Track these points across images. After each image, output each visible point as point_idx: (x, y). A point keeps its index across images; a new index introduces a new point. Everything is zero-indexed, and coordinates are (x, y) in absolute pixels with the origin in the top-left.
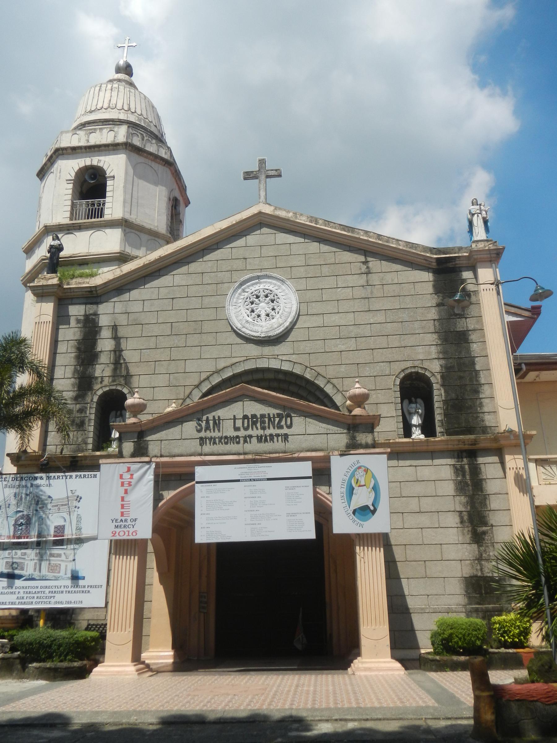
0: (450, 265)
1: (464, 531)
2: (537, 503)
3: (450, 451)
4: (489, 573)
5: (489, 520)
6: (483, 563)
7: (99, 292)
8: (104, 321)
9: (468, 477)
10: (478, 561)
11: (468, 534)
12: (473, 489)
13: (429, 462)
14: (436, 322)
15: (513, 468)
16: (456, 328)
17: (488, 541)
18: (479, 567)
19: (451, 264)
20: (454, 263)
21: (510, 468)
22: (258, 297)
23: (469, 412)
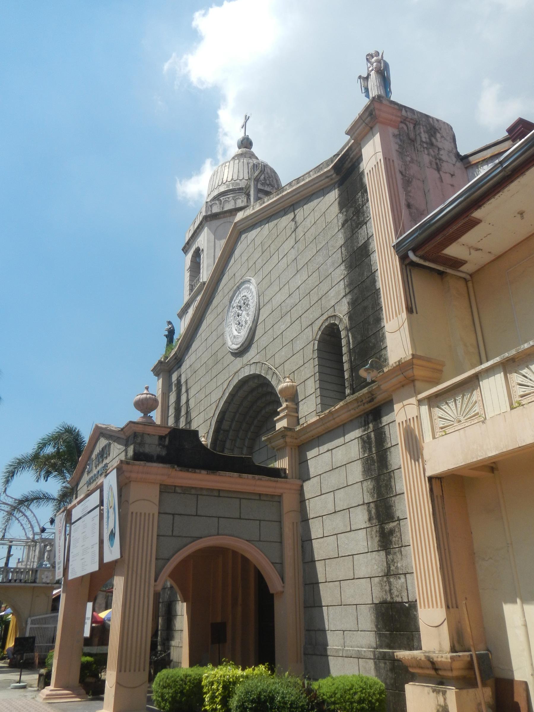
0: (347, 165)
1: (373, 533)
2: (429, 473)
3: (357, 418)
4: (398, 596)
5: (395, 511)
6: (392, 580)
7: (179, 356)
8: (183, 380)
9: (374, 449)
10: (387, 578)
11: (376, 536)
12: (378, 467)
13: (340, 441)
14: (343, 248)
15: (402, 422)
16: (359, 243)
17: (395, 545)
18: (387, 588)
19: (347, 163)
20: (349, 160)
21: (399, 424)
22: (240, 307)
23: (373, 353)
